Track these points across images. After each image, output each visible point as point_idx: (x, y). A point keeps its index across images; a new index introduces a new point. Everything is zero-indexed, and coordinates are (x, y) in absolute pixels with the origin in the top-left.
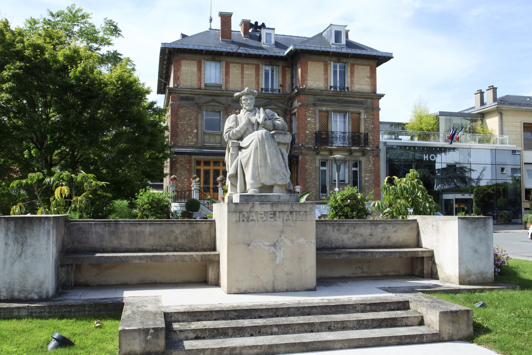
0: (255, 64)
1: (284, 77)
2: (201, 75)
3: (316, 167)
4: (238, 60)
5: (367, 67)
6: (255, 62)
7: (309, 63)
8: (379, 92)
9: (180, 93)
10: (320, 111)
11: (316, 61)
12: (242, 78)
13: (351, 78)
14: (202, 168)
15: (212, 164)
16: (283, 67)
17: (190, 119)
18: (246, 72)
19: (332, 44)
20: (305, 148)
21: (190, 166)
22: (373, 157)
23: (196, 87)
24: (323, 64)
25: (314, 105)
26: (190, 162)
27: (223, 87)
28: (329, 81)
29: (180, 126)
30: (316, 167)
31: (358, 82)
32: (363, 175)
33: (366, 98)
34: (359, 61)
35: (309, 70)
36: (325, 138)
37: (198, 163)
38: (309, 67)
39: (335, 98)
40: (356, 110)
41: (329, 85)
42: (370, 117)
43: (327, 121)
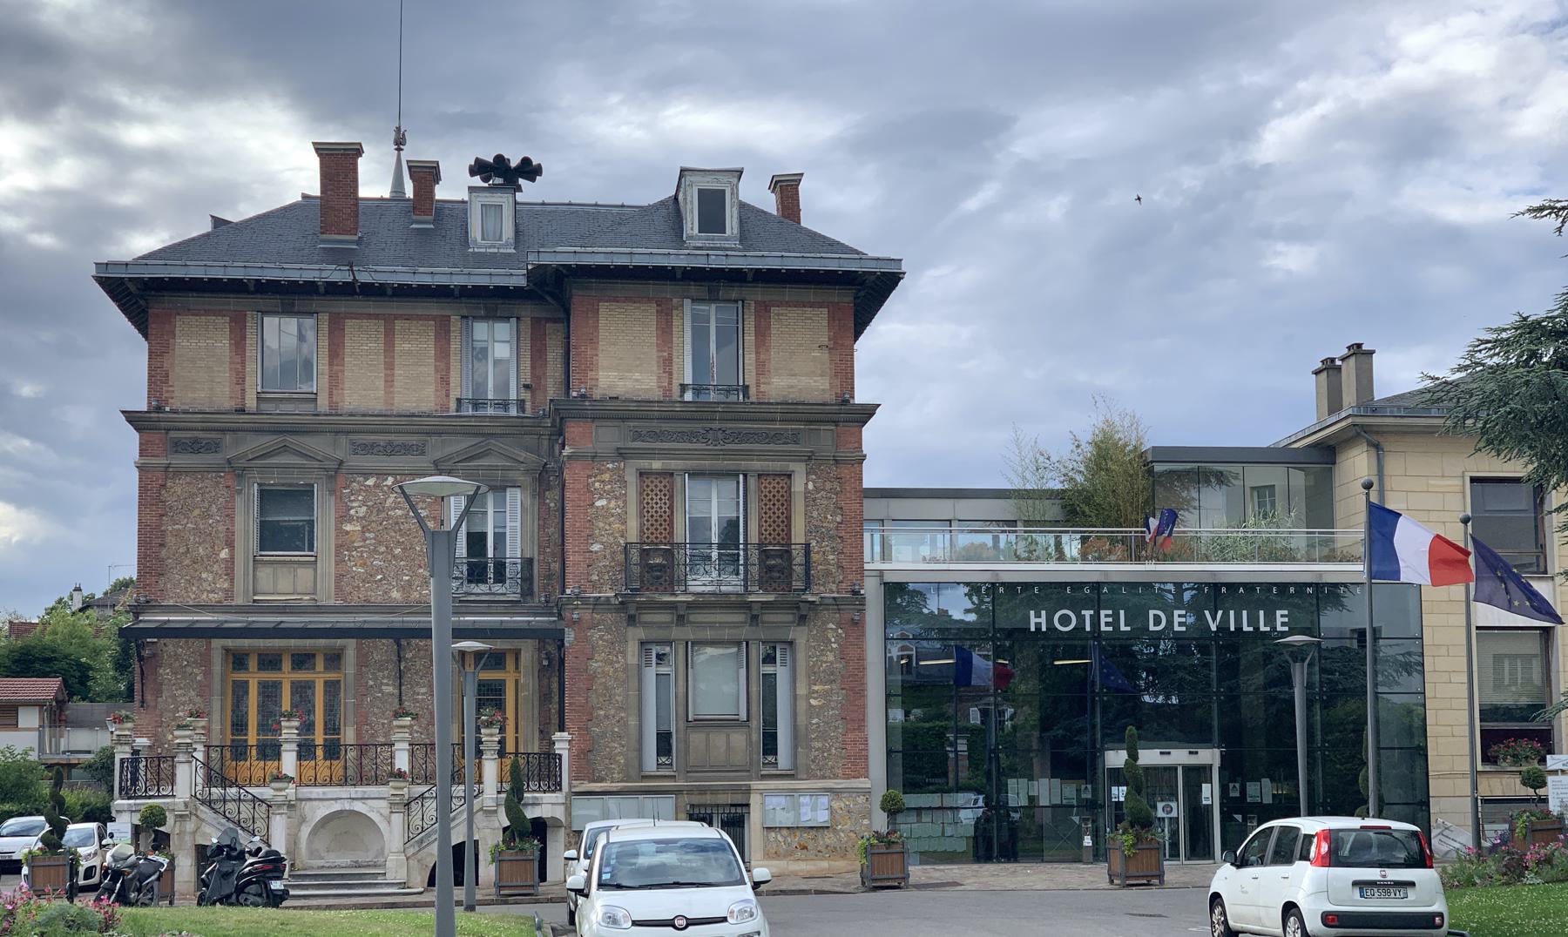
0: (434, 318)
1: (538, 356)
2: (243, 363)
3: (626, 669)
4: (372, 306)
5: (817, 311)
6: (434, 308)
7: (604, 308)
8: (861, 397)
9: (168, 430)
10: (642, 474)
11: (628, 299)
12: (390, 366)
13: (757, 353)
15: (287, 664)
16: (537, 323)
17: (206, 515)
18: (402, 346)
19: (691, 238)
20: (585, 601)
21: (208, 673)
22: (839, 625)
23: (228, 404)
24: (653, 308)
25: (622, 454)
26: (205, 661)
27: (323, 404)
28: (675, 367)
29: (170, 540)
30: (626, 669)
31: (788, 367)
32: (802, 690)
33: (810, 422)
34: (789, 293)
35: (602, 333)
36: (661, 567)
37: (238, 660)
38: (602, 322)
39: (698, 426)
40: (776, 466)
41: (676, 383)
42: (828, 486)
43: (671, 508)
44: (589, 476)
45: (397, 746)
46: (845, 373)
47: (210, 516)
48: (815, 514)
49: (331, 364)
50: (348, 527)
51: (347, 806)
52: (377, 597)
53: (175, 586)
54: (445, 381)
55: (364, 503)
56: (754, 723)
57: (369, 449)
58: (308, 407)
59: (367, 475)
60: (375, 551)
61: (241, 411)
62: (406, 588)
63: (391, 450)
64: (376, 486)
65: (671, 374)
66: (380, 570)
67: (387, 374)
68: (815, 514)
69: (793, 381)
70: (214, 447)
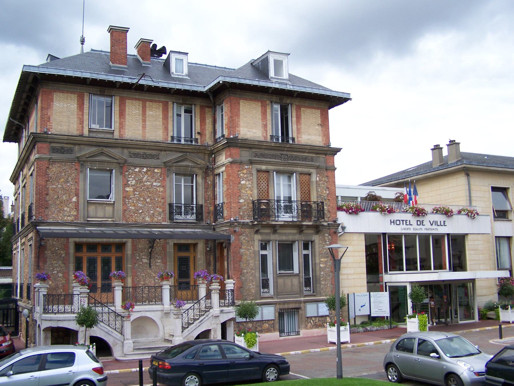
2: (83, 115)
4: (137, 95)
5: (316, 111)
7: (242, 103)
8: (334, 144)
10: (259, 171)
12: (144, 121)
13: (297, 125)
14: (85, 255)
17: (67, 181)
18: (149, 113)
19: (272, 78)
21: (67, 254)
22: (330, 235)
25: (251, 162)
26: (66, 248)
27: (116, 135)
29: (51, 192)
30: (254, 252)
33: (317, 154)
34: (307, 103)
35: (241, 113)
38: (241, 108)
39: (278, 153)
42: (324, 179)
44: (239, 171)
45: (164, 287)
46: (326, 135)
47: (68, 182)
48: (319, 190)
49: (120, 118)
50: (128, 189)
51: (144, 314)
52: (140, 220)
53: (53, 213)
54: (166, 129)
55: (134, 179)
56: (301, 275)
57: (136, 155)
58: (110, 136)
59: (135, 167)
60: (139, 200)
61: (82, 136)
62: (152, 216)
63: (145, 156)
64: (140, 171)
65: (267, 131)
66: (141, 208)
67: (143, 124)
68: (319, 190)
69: (309, 137)
70: (70, 151)
